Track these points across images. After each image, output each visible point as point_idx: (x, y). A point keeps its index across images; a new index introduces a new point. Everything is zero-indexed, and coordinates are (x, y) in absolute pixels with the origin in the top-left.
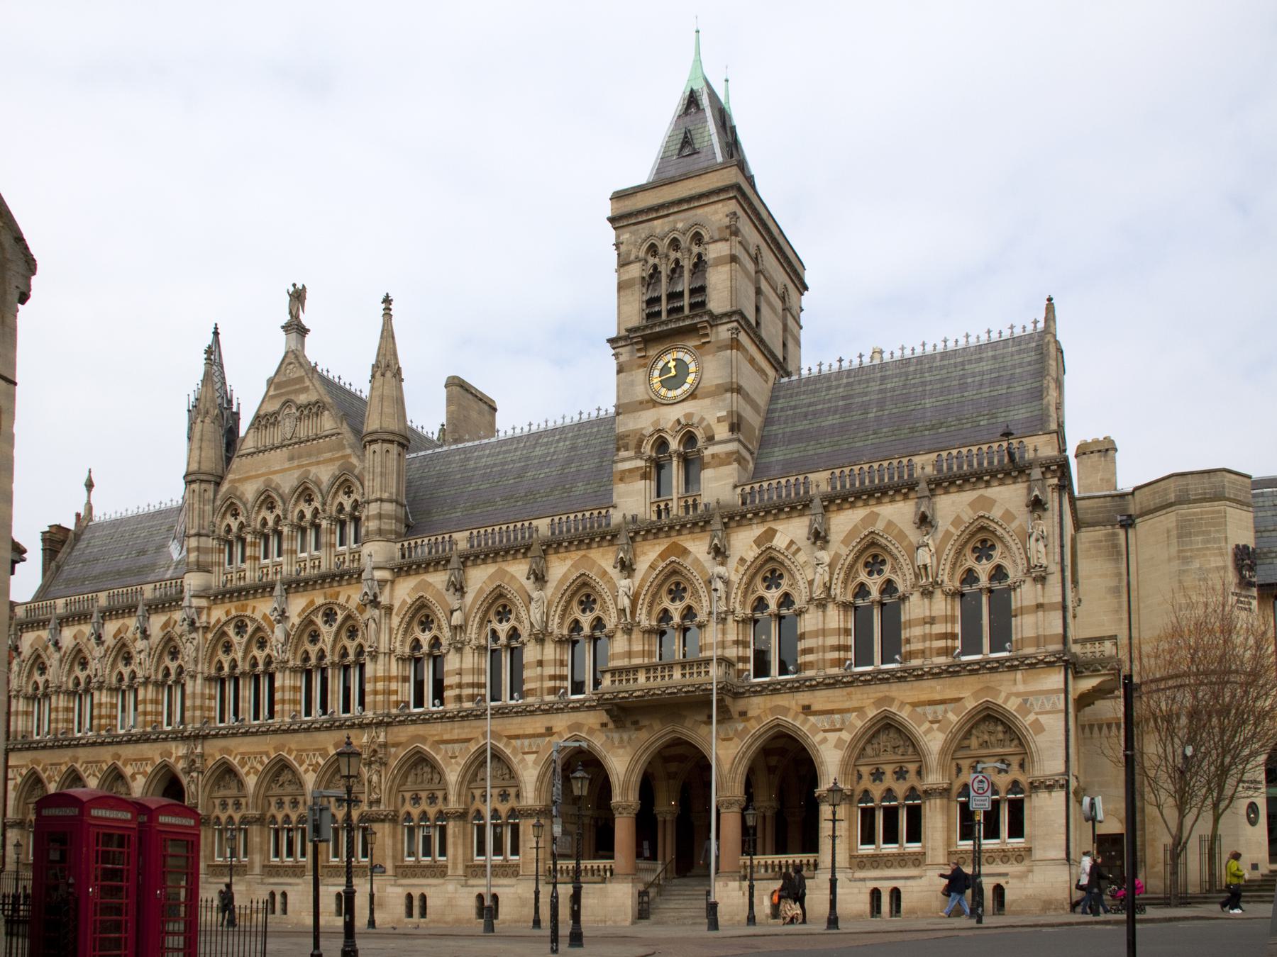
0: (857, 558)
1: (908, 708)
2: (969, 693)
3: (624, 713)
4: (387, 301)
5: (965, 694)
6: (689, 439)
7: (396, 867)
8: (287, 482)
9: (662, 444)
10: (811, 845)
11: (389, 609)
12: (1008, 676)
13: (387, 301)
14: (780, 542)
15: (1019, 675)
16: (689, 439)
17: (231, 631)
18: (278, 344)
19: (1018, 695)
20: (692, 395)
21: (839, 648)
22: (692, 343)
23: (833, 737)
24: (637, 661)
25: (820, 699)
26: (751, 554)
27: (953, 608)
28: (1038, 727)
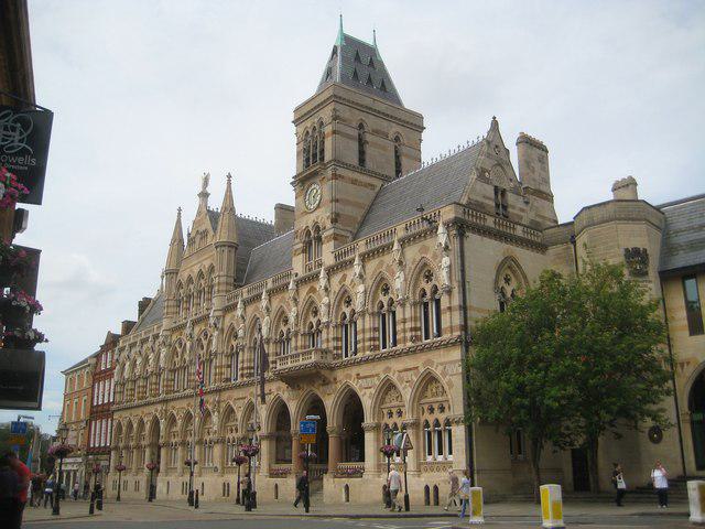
0: (377, 287)
1: (397, 373)
2: (419, 362)
3: (293, 379)
4: (229, 176)
5: (420, 364)
6: (317, 229)
7: (223, 468)
8: (196, 270)
9: (308, 233)
10: (362, 459)
11: (222, 330)
12: (437, 352)
13: (229, 176)
14: (348, 282)
15: (442, 352)
16: (317, 229)
17: (177, 345)
18: (197, 202)
19: (441, 364)
20: (318, 206)
21: (374, 339)
22: (317, 180)
23: (368, 391)
24: (299, 351)
25: (364, 370)
26: (337, 290)
27: (415, 312)
28: (450, 384)
